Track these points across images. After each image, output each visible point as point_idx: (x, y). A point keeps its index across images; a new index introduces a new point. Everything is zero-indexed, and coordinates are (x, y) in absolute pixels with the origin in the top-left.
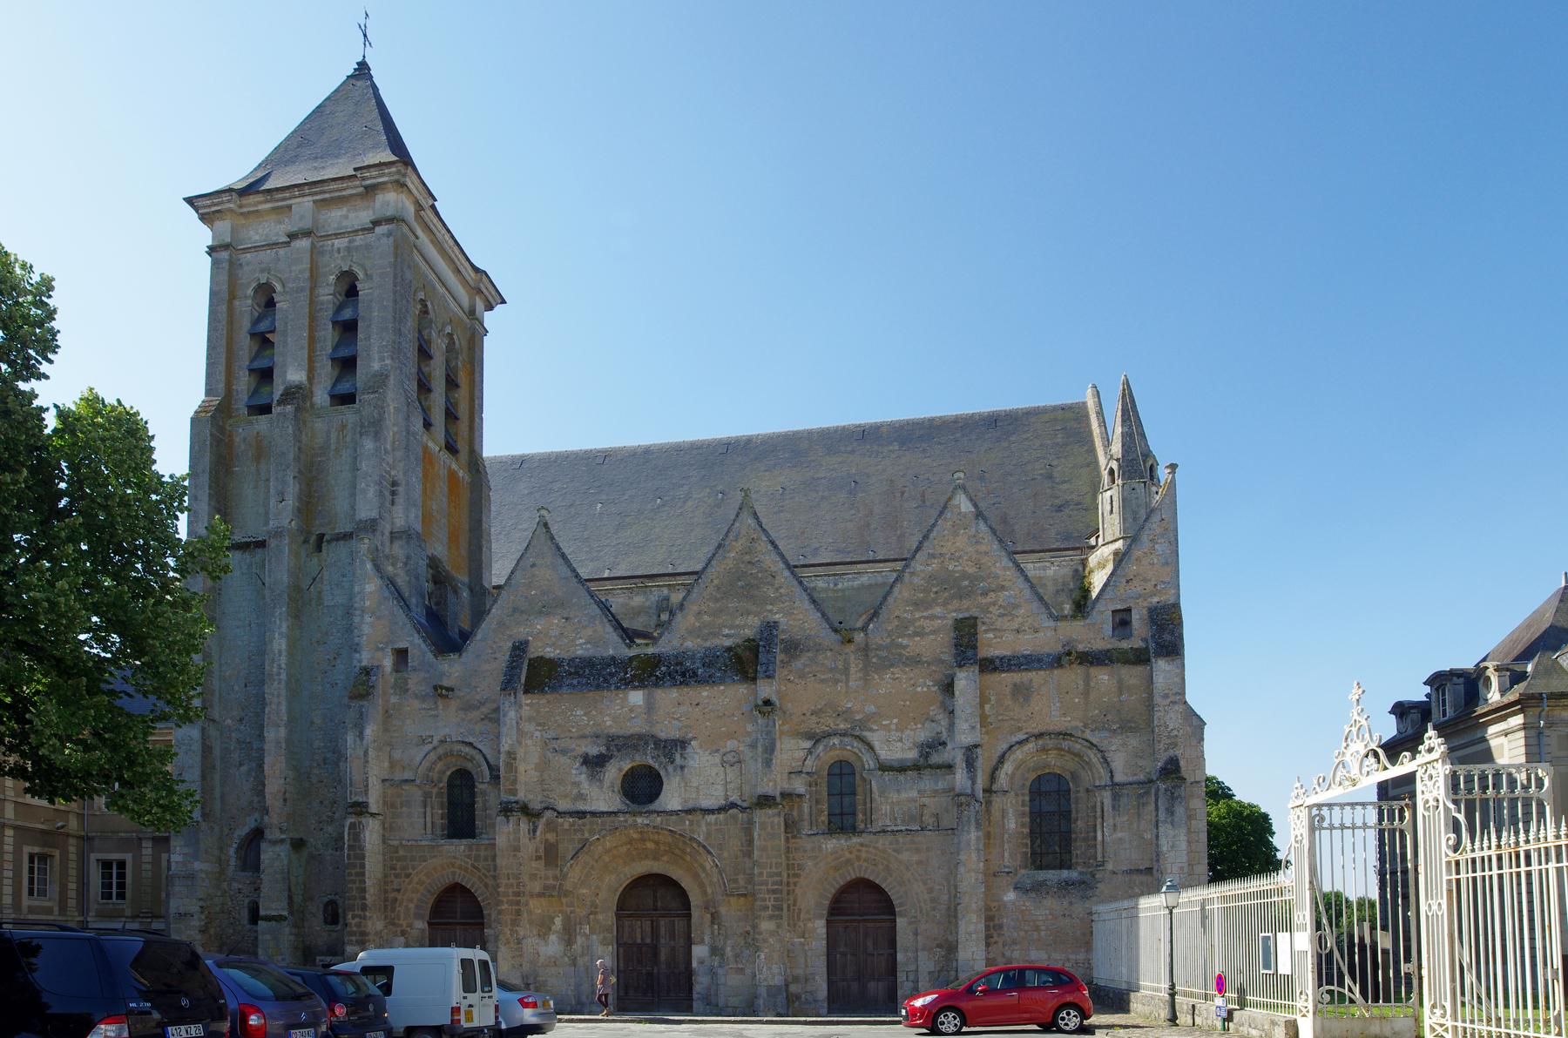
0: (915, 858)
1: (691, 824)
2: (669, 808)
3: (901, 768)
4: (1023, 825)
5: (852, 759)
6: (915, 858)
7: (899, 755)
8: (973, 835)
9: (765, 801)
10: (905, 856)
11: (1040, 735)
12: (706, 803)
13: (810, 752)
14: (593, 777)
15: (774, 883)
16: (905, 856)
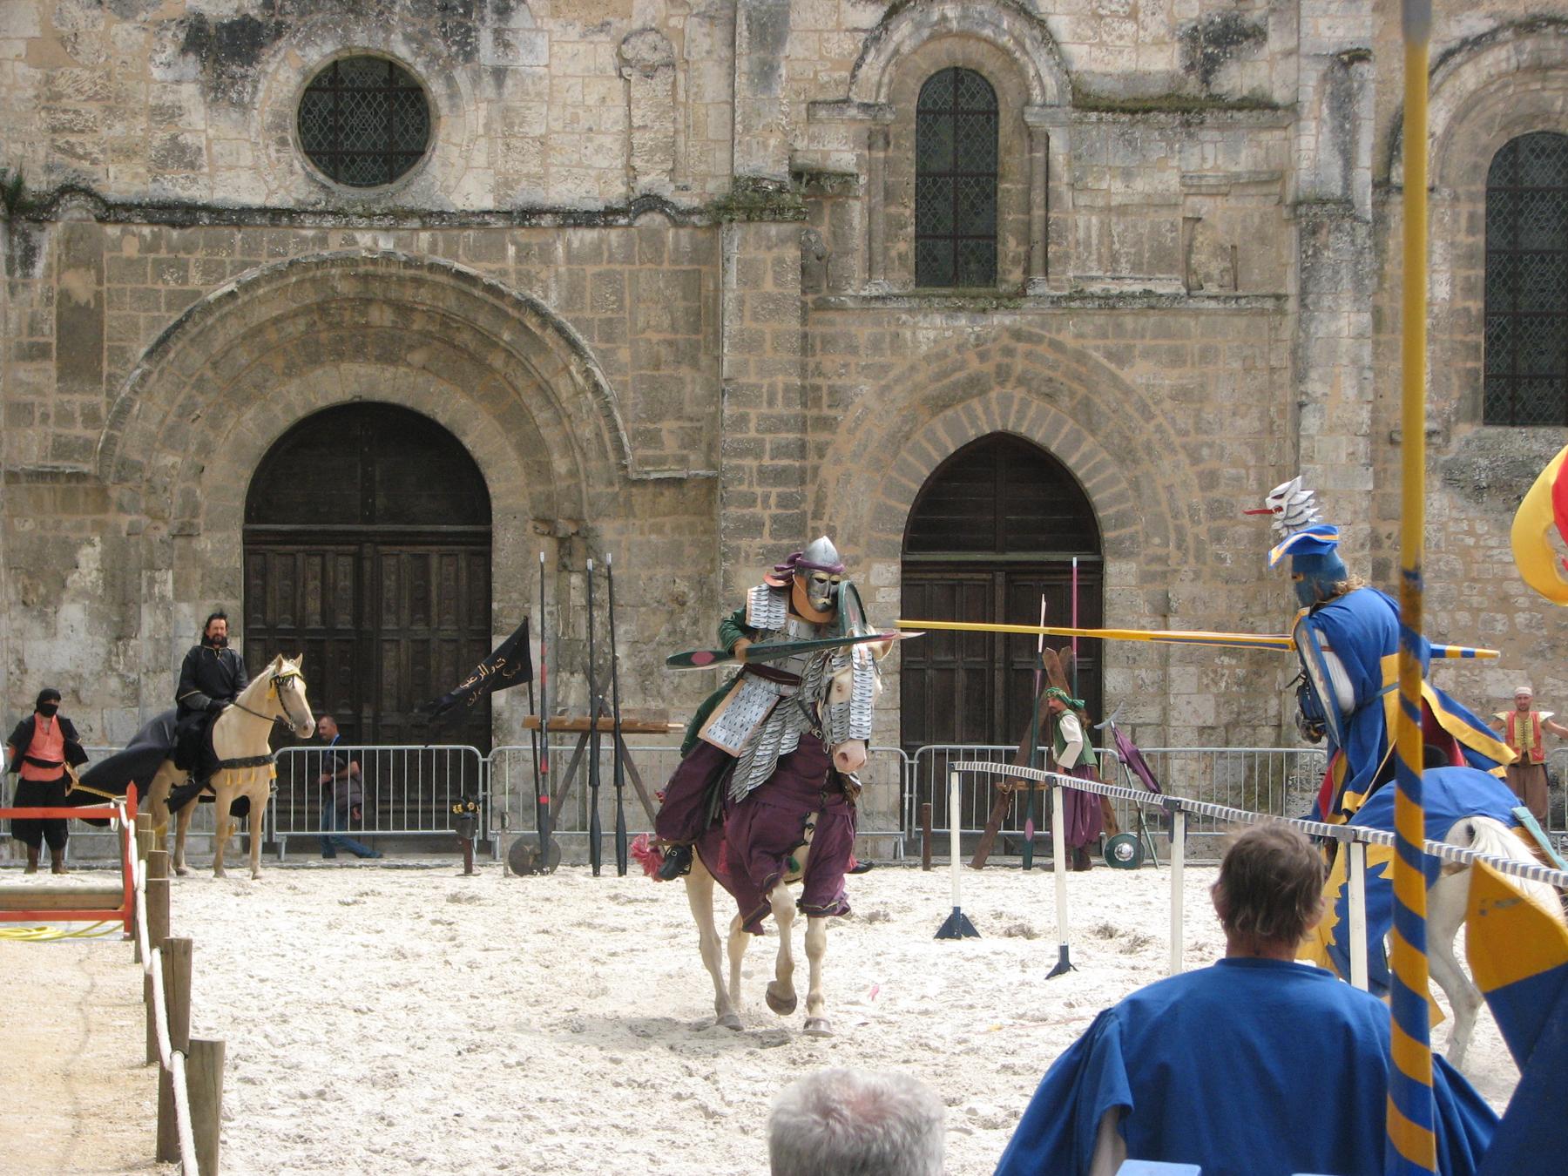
0: (1169, 379)
1: (524, 254)
2: (457, 202)
3: (1134, 107)
4: (1468, 290)
5: (991, 66)
6: (1169, 379)
7: (1124, 63)
8: (1343, 322)
9: (748, 202)
10: (1138, 374)
11: (1529, 26)
12: (563, 192)
13: (875, 37)
14: (218, 91)
15: (778, 452)
16: (1138, 374)
